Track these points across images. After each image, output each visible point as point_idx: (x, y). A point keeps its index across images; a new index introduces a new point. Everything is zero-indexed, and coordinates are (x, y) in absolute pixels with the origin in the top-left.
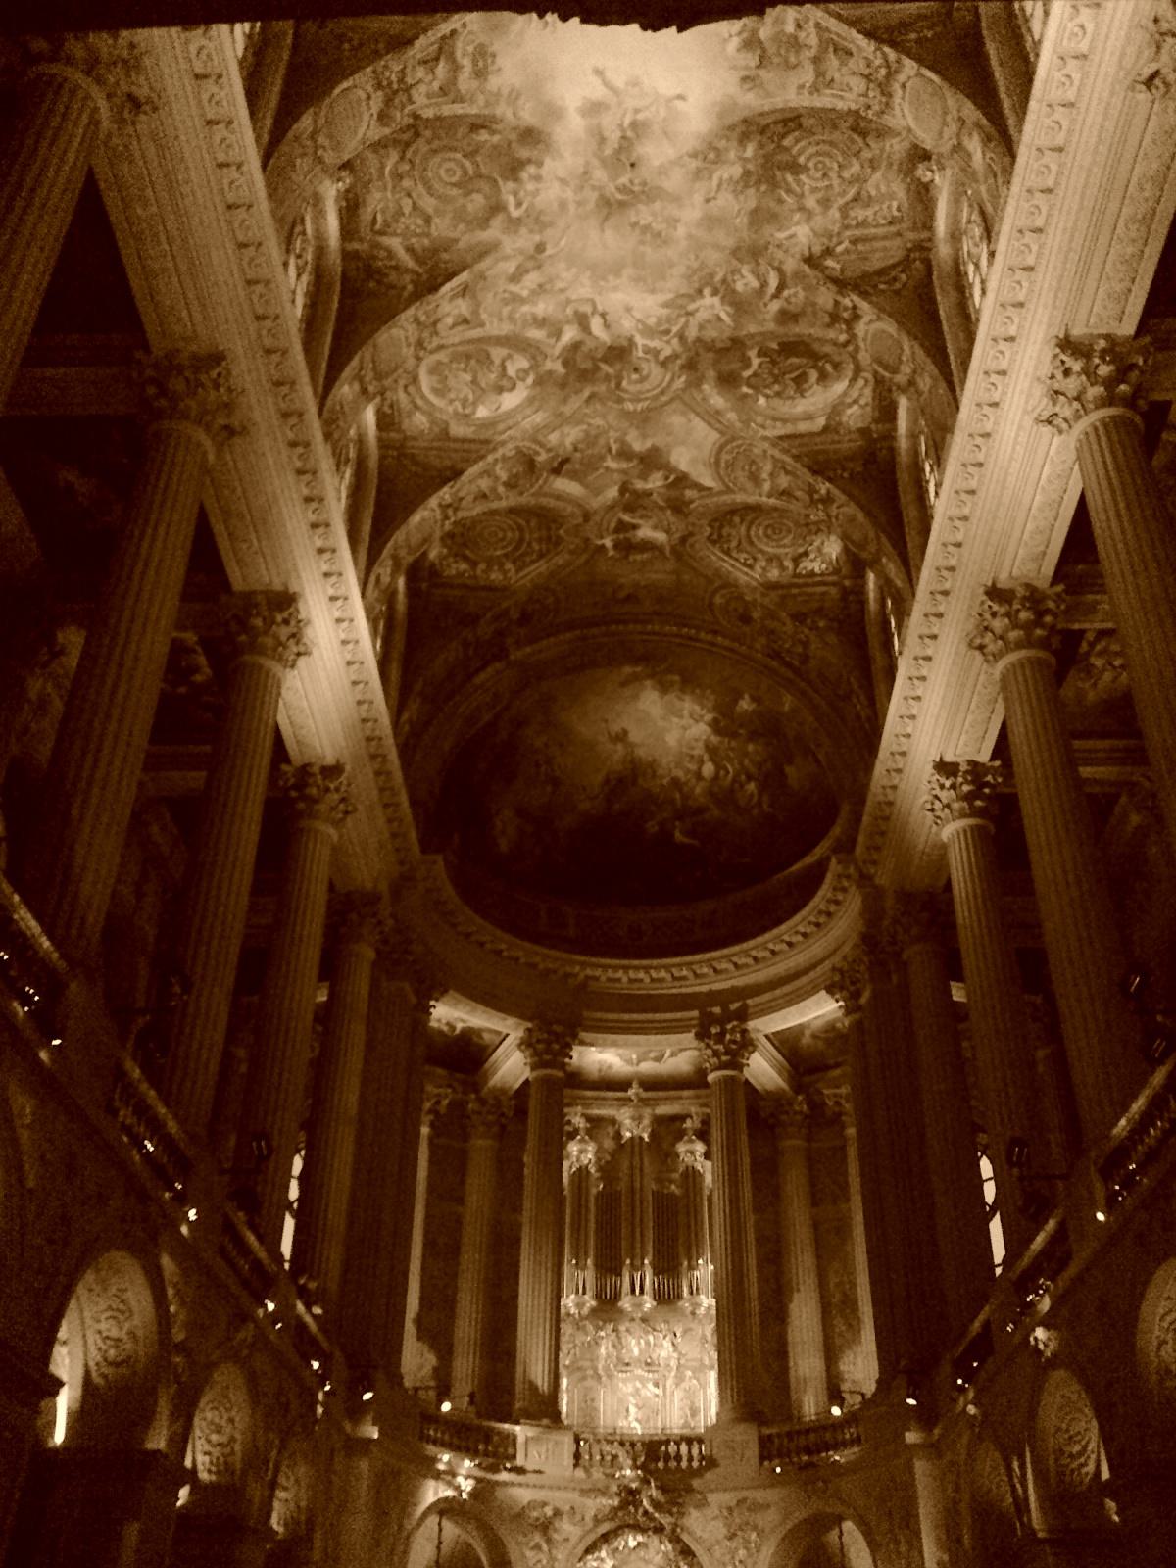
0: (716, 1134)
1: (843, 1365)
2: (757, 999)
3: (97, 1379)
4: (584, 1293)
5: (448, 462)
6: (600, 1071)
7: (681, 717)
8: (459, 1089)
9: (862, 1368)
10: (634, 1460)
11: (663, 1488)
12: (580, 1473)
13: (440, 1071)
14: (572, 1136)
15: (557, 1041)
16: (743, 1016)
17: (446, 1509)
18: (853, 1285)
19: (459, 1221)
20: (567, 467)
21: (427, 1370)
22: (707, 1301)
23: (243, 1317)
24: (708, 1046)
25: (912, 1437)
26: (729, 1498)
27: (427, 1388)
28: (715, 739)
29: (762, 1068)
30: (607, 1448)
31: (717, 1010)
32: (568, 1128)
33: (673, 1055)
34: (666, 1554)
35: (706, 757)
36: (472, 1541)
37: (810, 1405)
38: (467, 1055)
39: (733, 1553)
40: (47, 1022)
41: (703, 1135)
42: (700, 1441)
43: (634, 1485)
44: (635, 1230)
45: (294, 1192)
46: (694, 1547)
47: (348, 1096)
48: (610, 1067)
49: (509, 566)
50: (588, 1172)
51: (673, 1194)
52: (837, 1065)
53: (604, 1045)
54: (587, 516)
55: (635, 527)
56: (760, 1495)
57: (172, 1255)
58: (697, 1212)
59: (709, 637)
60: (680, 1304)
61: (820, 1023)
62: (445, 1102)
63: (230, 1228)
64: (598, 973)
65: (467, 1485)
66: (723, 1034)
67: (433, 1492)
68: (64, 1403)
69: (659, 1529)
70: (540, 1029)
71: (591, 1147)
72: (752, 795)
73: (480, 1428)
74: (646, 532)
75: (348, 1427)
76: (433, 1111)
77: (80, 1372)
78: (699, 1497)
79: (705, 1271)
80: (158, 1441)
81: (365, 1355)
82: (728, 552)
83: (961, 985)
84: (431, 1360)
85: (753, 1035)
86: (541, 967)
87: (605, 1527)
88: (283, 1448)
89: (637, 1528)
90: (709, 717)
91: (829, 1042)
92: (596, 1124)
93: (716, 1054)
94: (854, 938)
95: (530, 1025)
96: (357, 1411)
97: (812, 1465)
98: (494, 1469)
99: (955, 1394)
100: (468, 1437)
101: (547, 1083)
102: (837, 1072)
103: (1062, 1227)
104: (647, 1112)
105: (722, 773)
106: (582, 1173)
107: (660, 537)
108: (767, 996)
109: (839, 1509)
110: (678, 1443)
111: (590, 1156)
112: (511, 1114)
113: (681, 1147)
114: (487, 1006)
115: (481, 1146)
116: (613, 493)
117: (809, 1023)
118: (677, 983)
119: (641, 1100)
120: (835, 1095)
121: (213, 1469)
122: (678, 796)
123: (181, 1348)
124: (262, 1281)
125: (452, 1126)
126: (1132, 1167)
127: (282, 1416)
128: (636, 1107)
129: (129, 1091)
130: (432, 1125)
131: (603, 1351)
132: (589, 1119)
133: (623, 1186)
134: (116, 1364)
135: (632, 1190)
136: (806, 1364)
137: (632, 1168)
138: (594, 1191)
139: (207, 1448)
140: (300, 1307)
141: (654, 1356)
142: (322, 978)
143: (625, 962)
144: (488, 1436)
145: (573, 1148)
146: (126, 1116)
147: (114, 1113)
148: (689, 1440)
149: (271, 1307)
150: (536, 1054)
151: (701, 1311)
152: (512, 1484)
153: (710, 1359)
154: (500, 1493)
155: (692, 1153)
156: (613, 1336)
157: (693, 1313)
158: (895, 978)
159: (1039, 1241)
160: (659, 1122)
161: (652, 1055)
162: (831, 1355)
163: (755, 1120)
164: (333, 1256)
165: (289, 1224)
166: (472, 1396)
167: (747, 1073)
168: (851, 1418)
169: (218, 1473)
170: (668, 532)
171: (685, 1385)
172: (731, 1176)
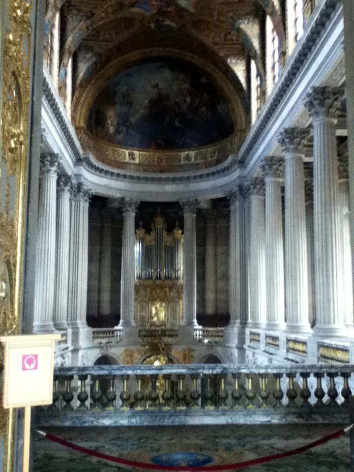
5: (89, 10)
20: (136, 5)
28: (191, 89)
35: (188, 95)
49: (112, 32)
54: (144, 18)
55: (163, 22)
59: (191, 54)
72: (204, 112)
74: (167, 22)
82: (200, 31)
90: (190, 82)
105: (194, 102)
107: (173, 24)
116: (155, 11)
122: (177, 110)
170: (176, 23)
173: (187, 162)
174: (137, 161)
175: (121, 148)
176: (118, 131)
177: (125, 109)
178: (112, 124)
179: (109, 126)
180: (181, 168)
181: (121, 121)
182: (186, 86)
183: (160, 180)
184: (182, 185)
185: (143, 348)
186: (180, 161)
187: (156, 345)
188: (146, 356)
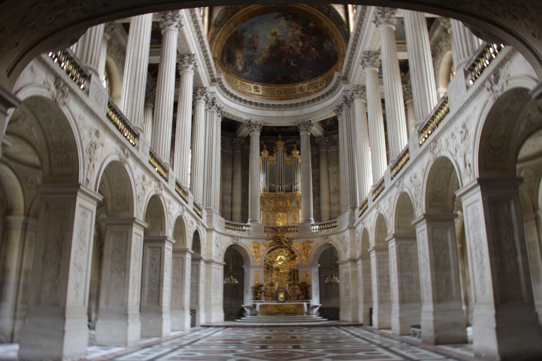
7: (292, 28)
28: (303, 34)
35: (300, 40)
90: (301, 28)
173: (302, 93)
174: (261, 93)
175: (248, 82)
176: (245, 70)
177: (250, 53)
178: (240, 64)
179: (238, 64)
180: (297, 97)
181: (248, 62)
182: (298, 32)
183: (280, 106)
184: (298, 111)
185: (269, 242)
186: (295, 92)
187: (279, 239)
188: (272, 248)
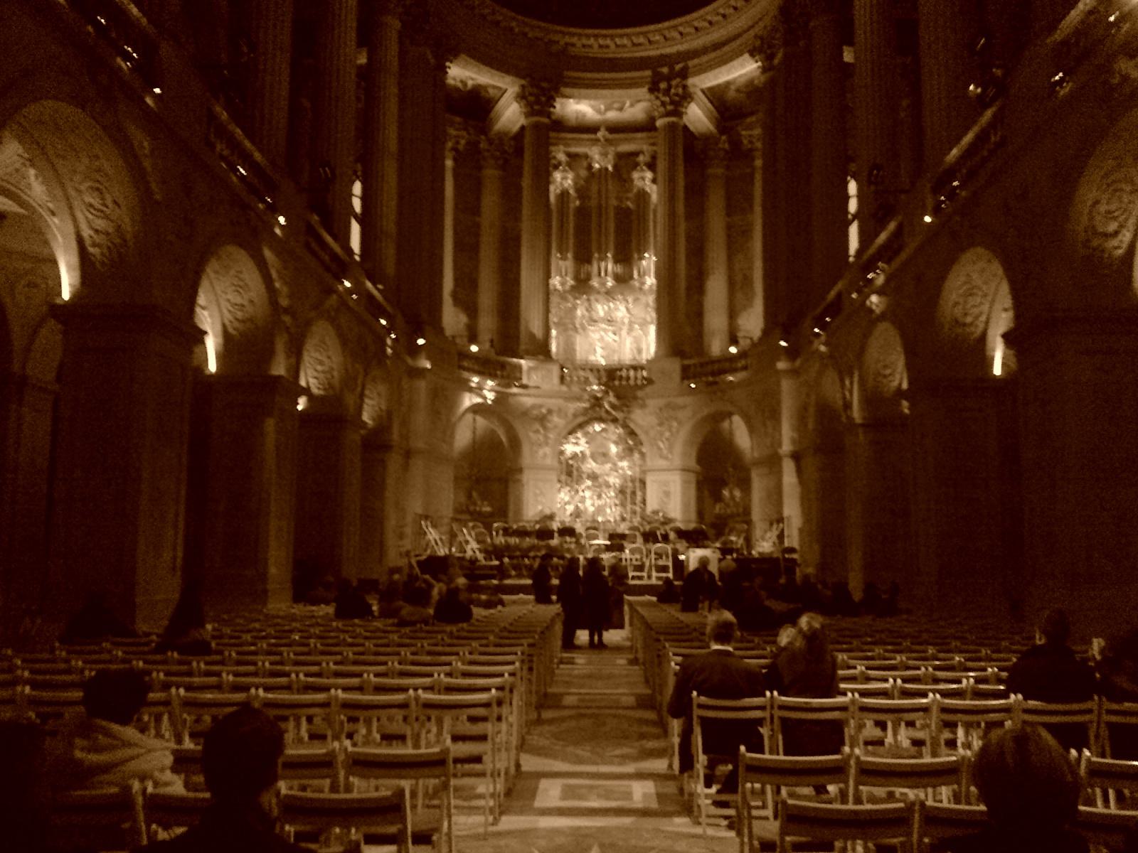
0: (662, 165)
1: (738, 319)
2: (696, 61)
3: (231, 330)
4: (566, 275)
6: (577, 118)
8: (472, 131)
9: (753, 322)
10: (599, 379)
11: (618, 397)
12: (564, 388)
13: (458, 119)
14: (556, 167)
15: (544, 95)
16: (684, 74)
17: (476, 409)
18: (751, 268)
19: (478, 226)
21: (461, 326)
22: (650, 281)
23: (330, 291)
24: (657, 98)
25: (781, 365)
26: (661, 402)
27: (461, 336)
29: (697, 115)
30: (582, 373)
31: (665, 70)
32: (554, 162)
33: (632, 105)
34: (619, 435)
36: (497, 429)
37: (716, 347)
38: (477, 105)
39: (662, 434)
40: (148, 72)
41: (652, 166)
42: (642, 368)
43: (599, 395)
44: (602, 231)
45: (357, 204)
46: (638, 431)
47: (390, 136)
48: (584, 115)
50: (568, 193)
51: (628, 208)
52: (752, 113)
53: (579, 98)
56: (680, 401)
57: (271, 248)
58: (645, 221)
60: (632, 282)
61: (743, 80)
62: (463, 142)
63: (311, 231)
64: (575, 40)
65: (491, 396)
66: (670, 87)
67: (469, 400)
68: (211, 345)
69: (615, 420)
70: (532, 86)
71: (570, 175)
73: (498, 362)
75: (410, 361)
76: (455, 149)
77: (219, 328)
78: (640, 402)
79: (649, 261)
80: (279, 368)
81: (417, 315)
83: (851, 49)
84: (464, 319)
85: (692, 90)
86: (530, 35)
87: (581, 419)
88: (366, 374)
89: (601, 420)
91: (749, 94)
92: (573, 157)
93: (663, 104)
94: (774, 11)
95: (523, 82)
96: (415, 351)
97: (715, 383)
98: (509, 386)
99: (812, 338)
100: (487, 367)
101: (536, 127)
102: (753, 119)
103: (900, 228)
104: (611, 150)
106: (564, 195)
108: (705, 59)
109: (730, 408)
110: (628, 370)
111: (570, 181)
112: (511, 151)
113: (636, 175)
114: (492, 67)
115: (491, 174)
117: (735, 80)
118: (635, 49)
119: (607, 140)
120: (750, 136)
121: (321, 387)
123: (286, 311)
124: (341, 266)
125: (470, 161)
126: (956, 183)
127: (364, 353)
128: (603, 146)
129: (222, 132)
130: (455, 160)
131: (579, 312)
132: (569, 155)
133: (593, 203)
134: (243, 321)
135: (600, 207)
136: (716, 321)
137: (599, 192)
138: (572, 205)
139: (316, 374)
140: (369, 285)
141: (613, 315)
142: (360, 44)
143: (596, 31)
144: (503, 366)
145: (557, 176)
146: (222, 150)
147: (213, 147)
148: (635, 368)
149: (347, 284)
150: (529, 104)
151: (646, 287)
152: (521, 395)
153: (651, 316)
154: (511, 400)
155: (644, 180)
156: (586, 304)
157: (641, 289)
158: (802, 43)
159: (883, 237)
160: (620, 157)
161: (616, 105)
162: (733, 314)
163: (690, 154)
164: (389, 252)
165: (355, 229)
166: (492, 341)
167: (686, 120)
168: (742, 355)
169: (325, 389)
171: (634, 334)
172: (671, 197)
